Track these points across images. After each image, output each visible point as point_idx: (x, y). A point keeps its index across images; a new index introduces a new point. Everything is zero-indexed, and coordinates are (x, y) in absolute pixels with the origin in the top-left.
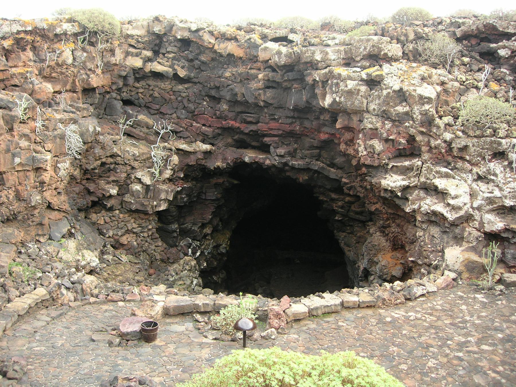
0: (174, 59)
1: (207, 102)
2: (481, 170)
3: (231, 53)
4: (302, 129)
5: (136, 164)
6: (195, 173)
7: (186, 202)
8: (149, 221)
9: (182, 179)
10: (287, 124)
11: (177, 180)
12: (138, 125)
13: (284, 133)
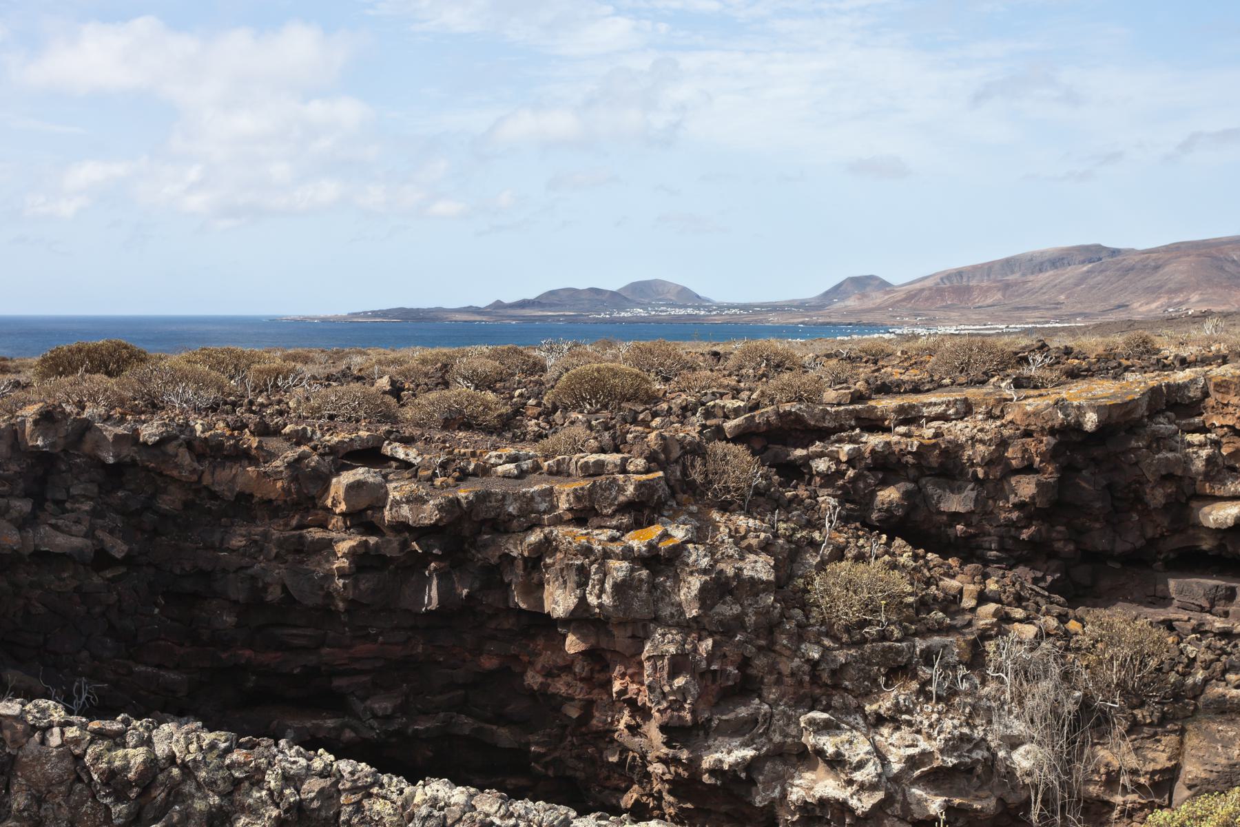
0: (94, 513)
2: (884, 705)
3: (248, 491)
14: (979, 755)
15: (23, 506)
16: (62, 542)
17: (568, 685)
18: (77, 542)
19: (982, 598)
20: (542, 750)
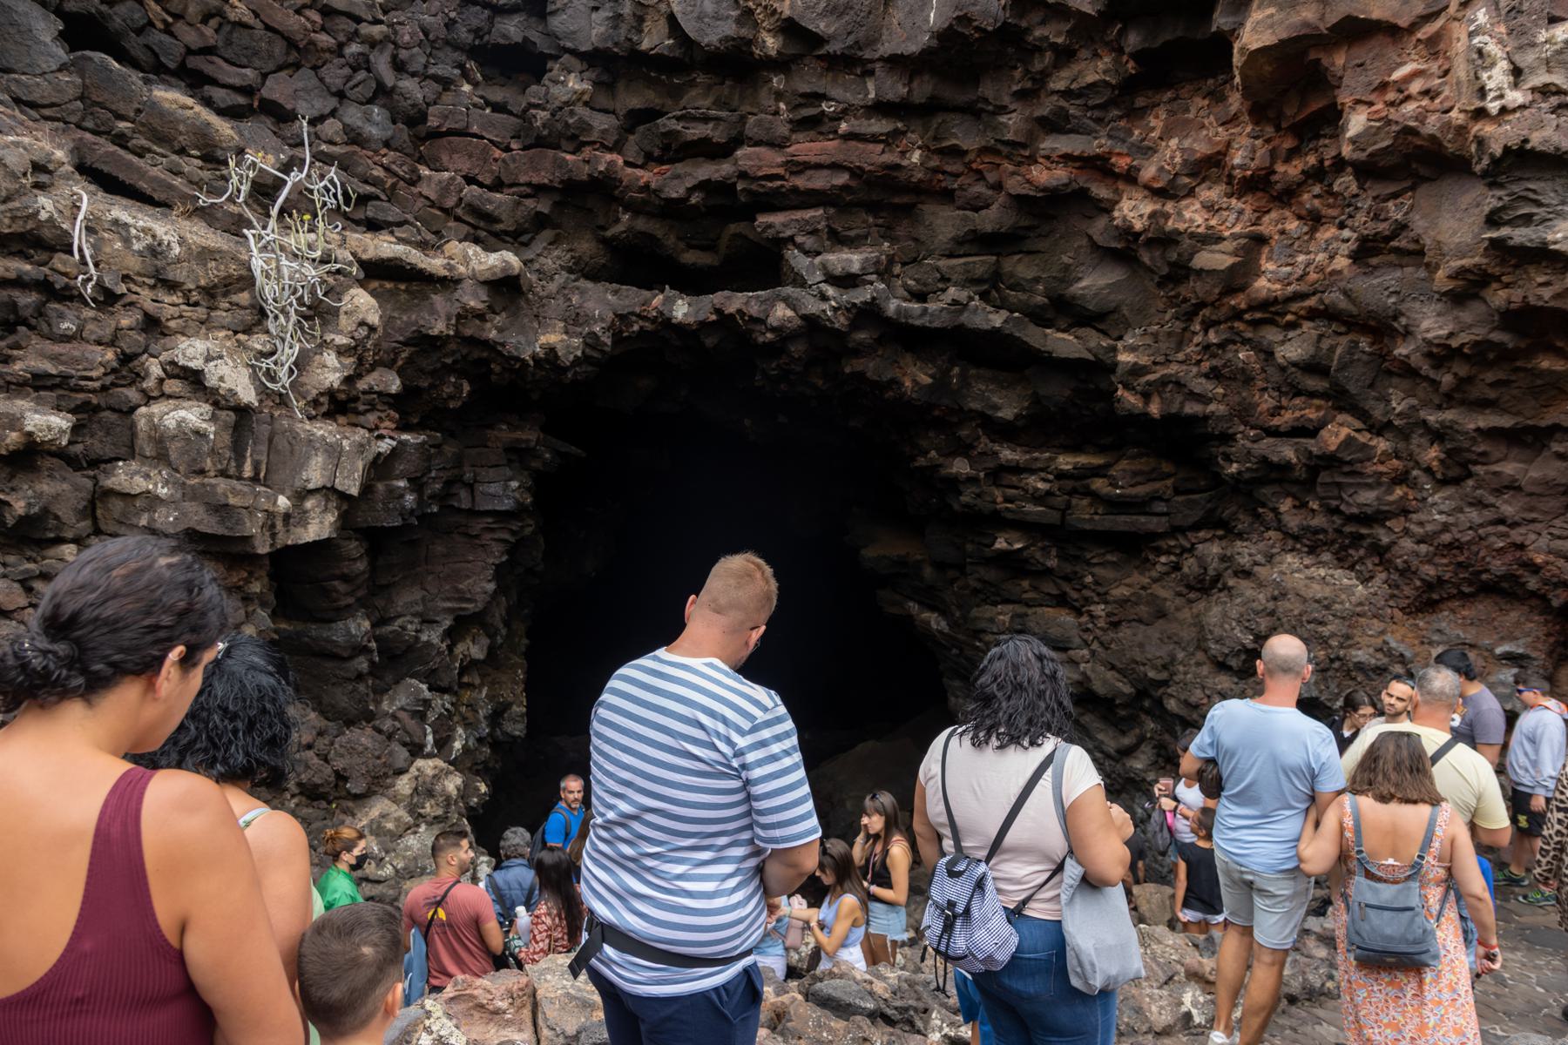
1: (476, 85)
4: (934, 162)
5: (168, 306)
6: (445, 384)
7: (412, 511)
8: (247, 599)
9: (394, 401)
10: (874, 139)
11: (372, 407)
12: (161, 139)
13: (853, 184)
17: (1210, 208)
20: (1144, 360)
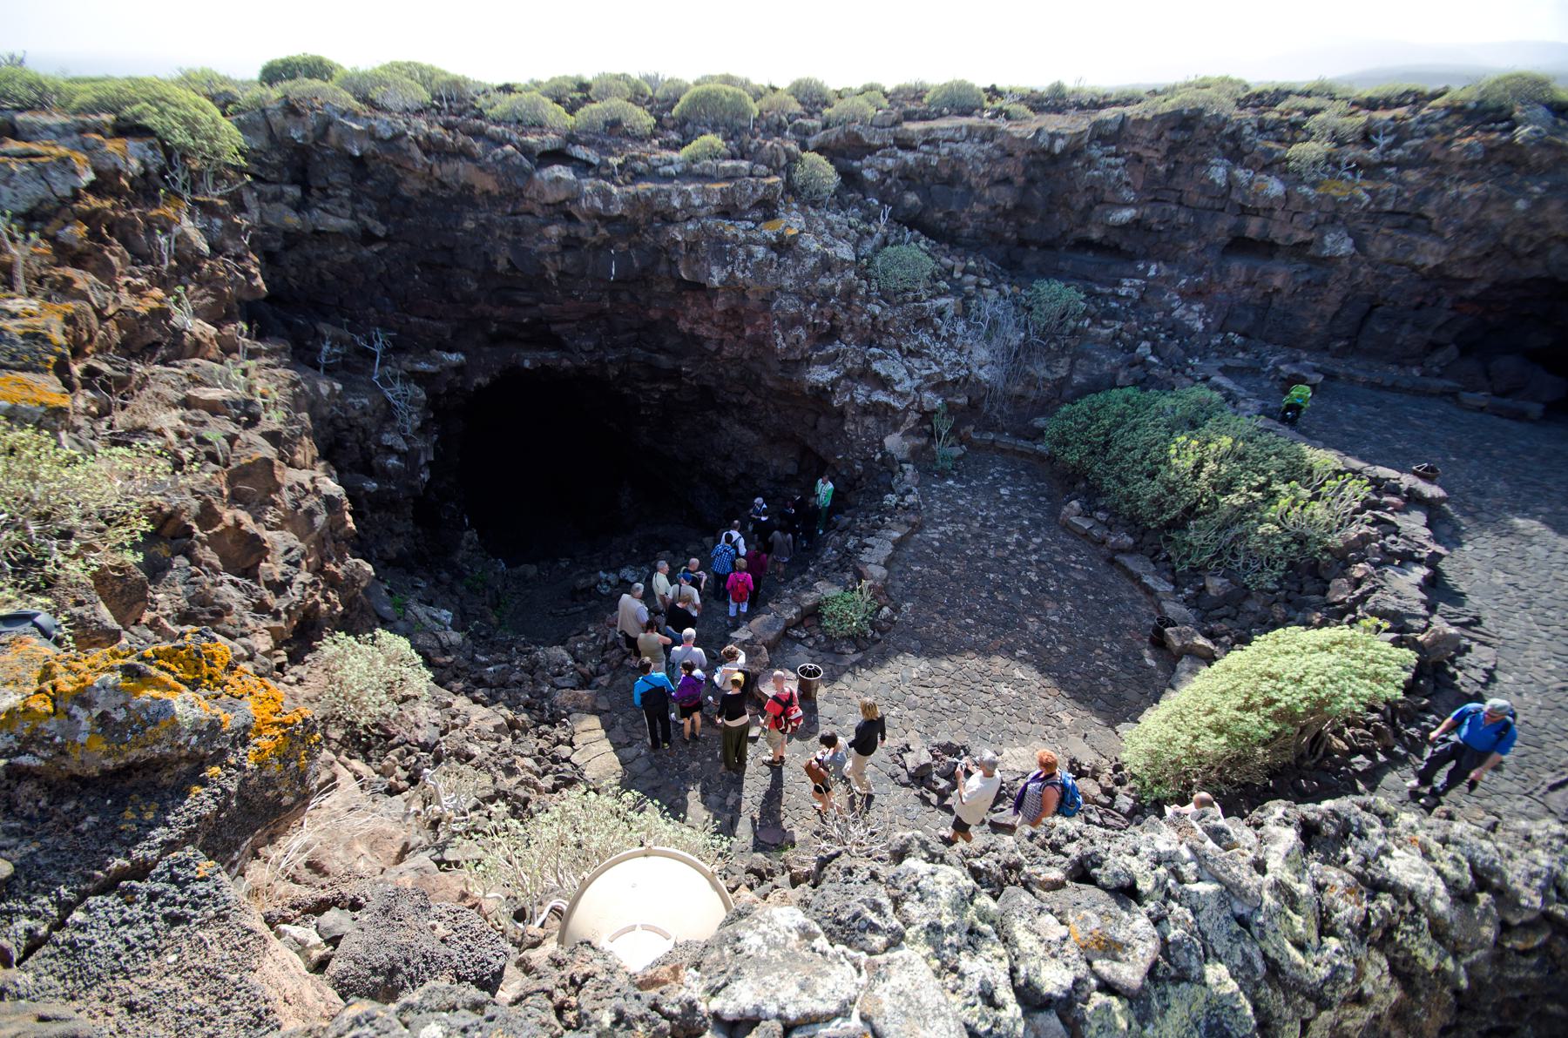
14: (964, 372)
15: (293, 192)
16: (334, 223)
18: (346, 223)
19: (965, 272)
